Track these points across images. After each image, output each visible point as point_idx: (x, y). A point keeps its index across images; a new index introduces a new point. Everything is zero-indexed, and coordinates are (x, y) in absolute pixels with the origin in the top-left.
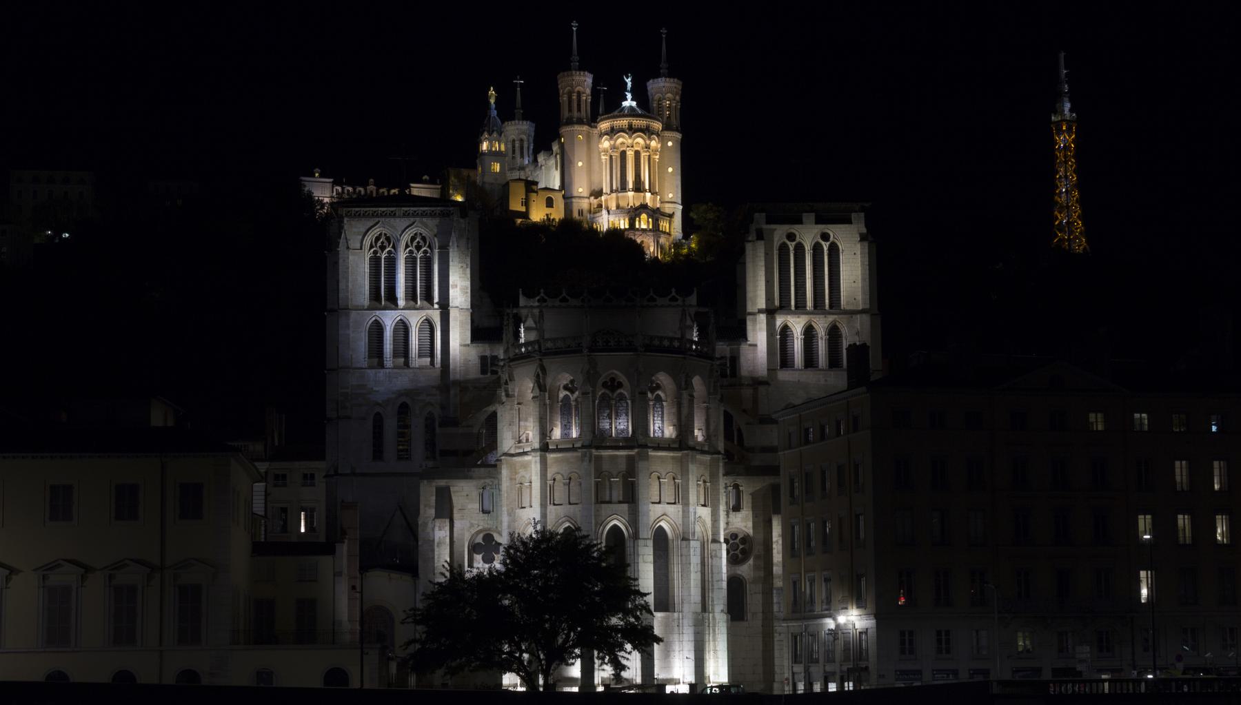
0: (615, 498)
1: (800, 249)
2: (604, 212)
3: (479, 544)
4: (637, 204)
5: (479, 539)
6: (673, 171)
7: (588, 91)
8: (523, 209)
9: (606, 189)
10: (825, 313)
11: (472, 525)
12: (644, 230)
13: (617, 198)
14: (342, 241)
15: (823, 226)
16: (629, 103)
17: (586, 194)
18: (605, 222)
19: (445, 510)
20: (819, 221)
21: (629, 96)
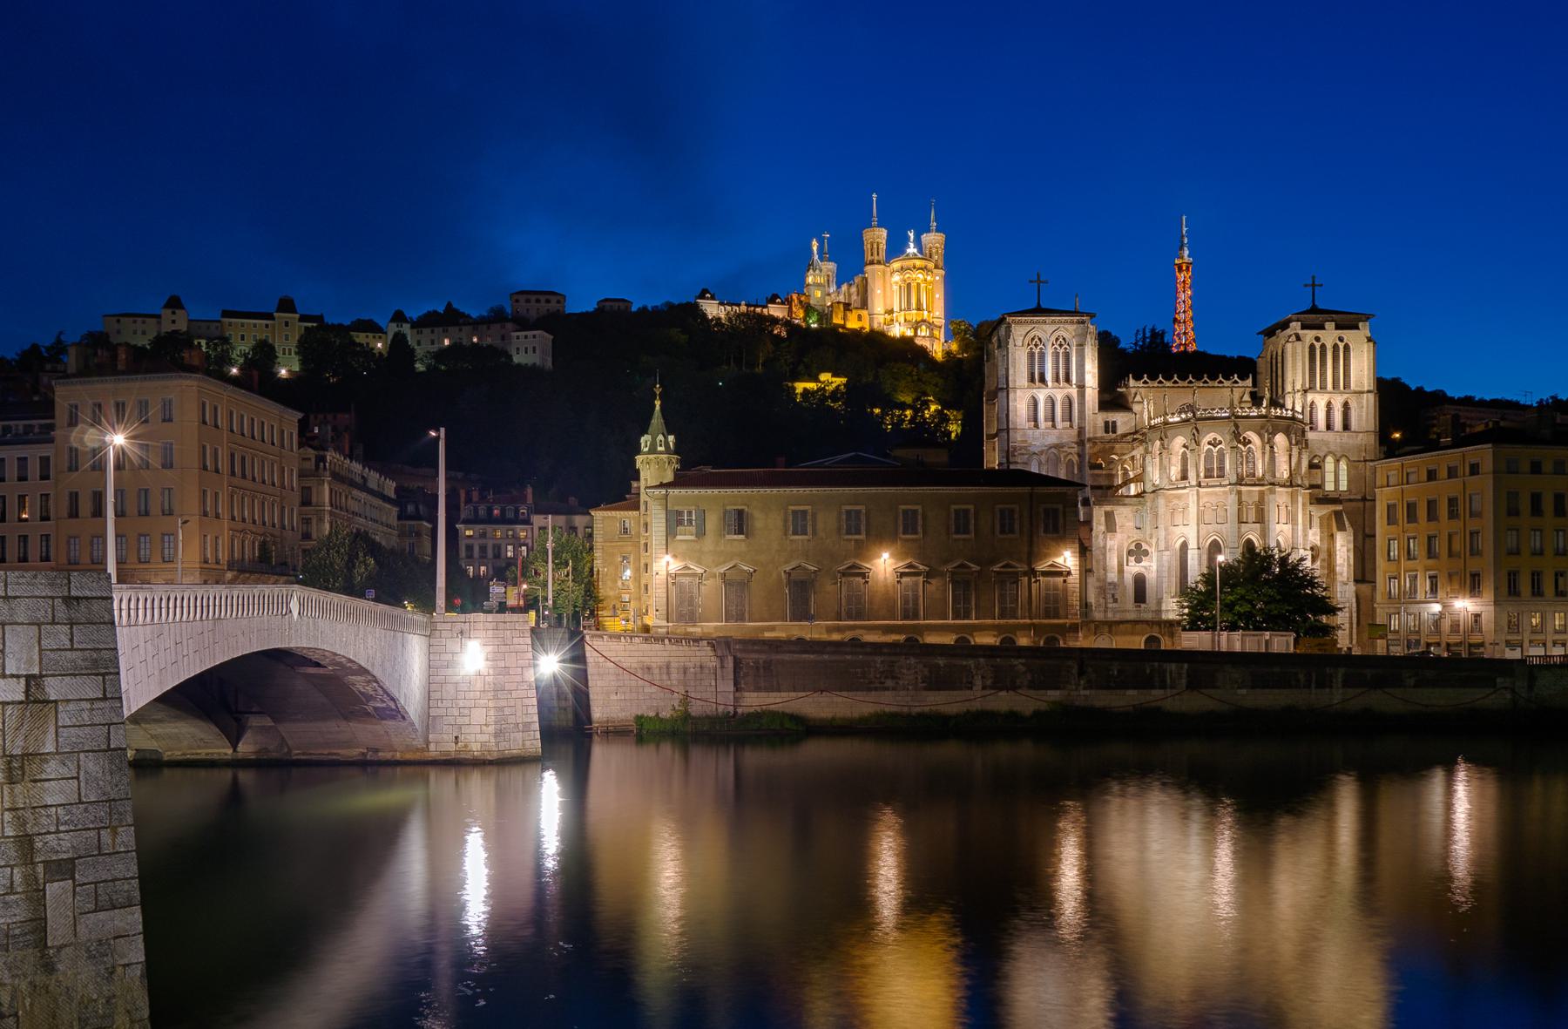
0: (1250, 521)
1: (1323, 347)
2: (897, 324)
3: (1132, 550)
4: (919, 319)
5: (1133, 547)
6: (939, 296)
7: (884, 242)
8: (842, 322)
9: (896, 308)
10: (1342, 393)
11: (1129, 537)
12: (924, 337)
13: (905, 315)
14: (1011, 341)
15: (1340, 331)
16: (912, 250)
17: (883, 312)
18: (896, 331)
19: (1111, 526)
20: (1338, 327)
21: (912, 245)
